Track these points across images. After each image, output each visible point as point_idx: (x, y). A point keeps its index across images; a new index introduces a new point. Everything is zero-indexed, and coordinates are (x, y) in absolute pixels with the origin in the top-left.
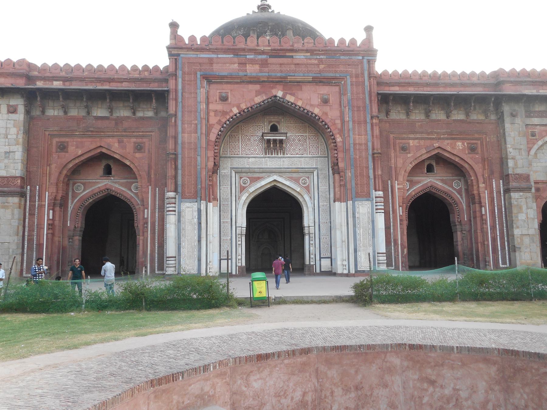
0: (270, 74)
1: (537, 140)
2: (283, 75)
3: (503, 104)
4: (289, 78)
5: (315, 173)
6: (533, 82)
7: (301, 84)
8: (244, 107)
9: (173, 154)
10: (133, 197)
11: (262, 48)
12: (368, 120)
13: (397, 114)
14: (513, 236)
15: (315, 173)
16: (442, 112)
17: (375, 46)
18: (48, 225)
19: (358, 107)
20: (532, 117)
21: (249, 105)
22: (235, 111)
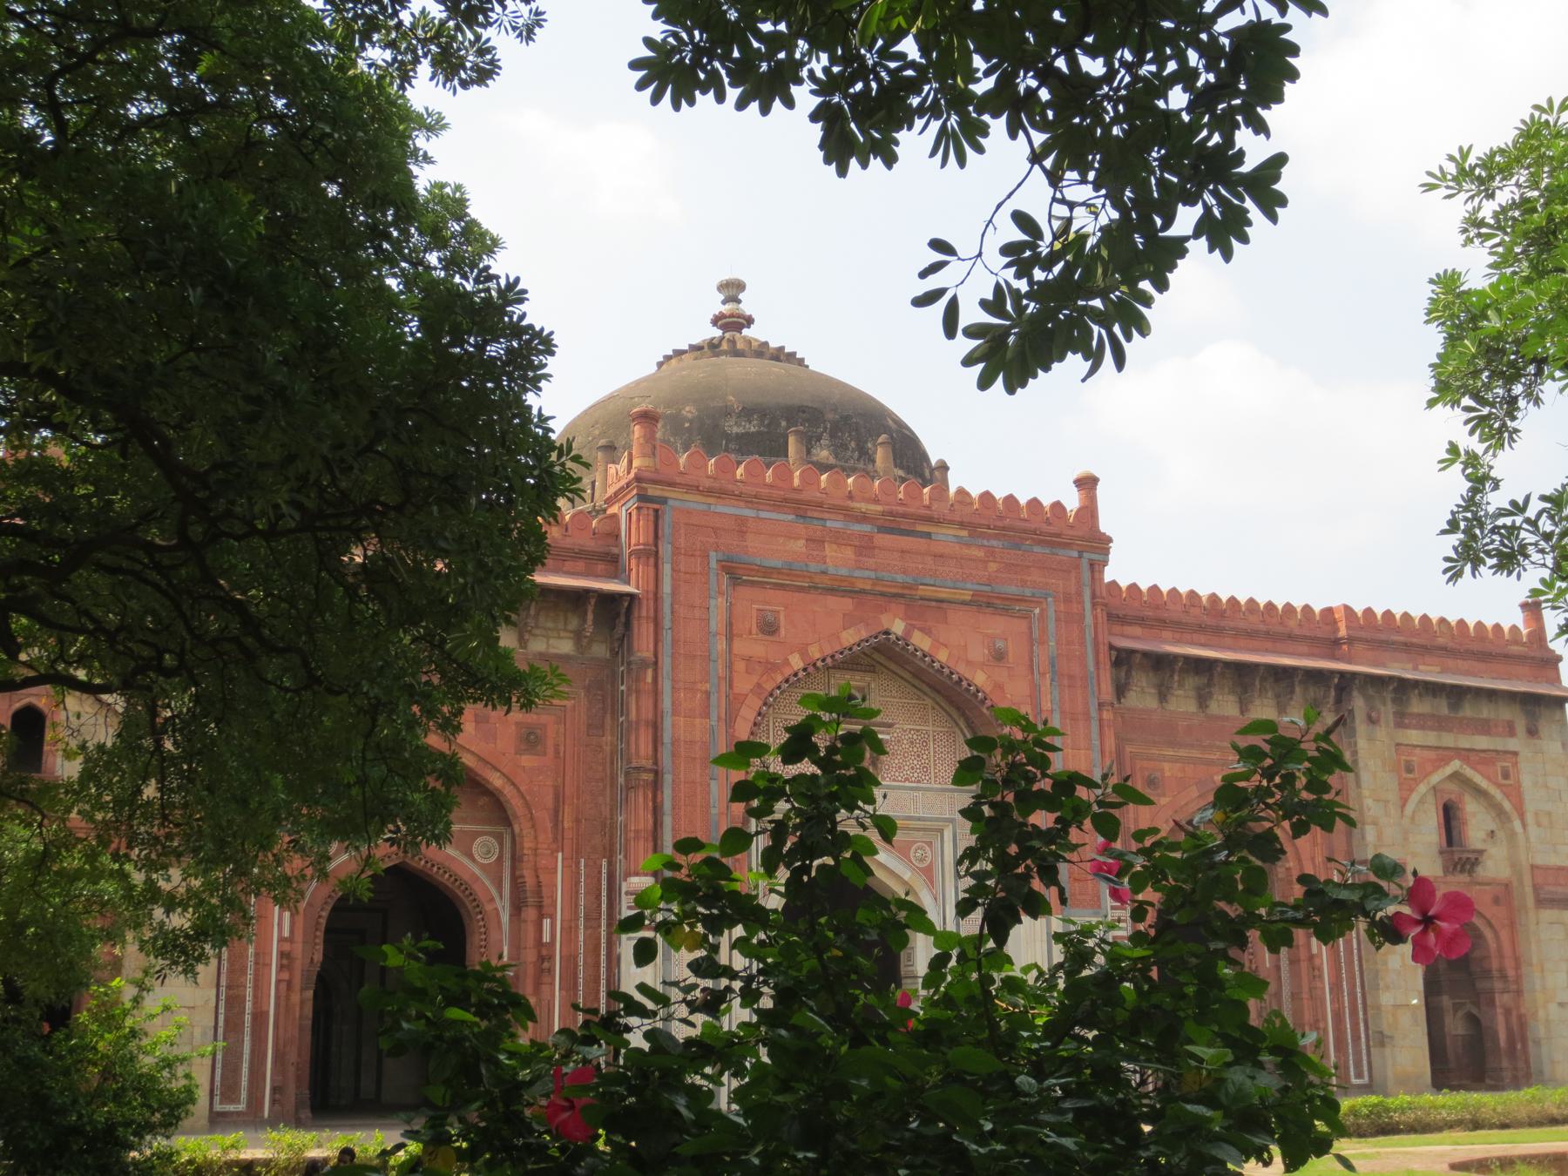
0: (880, 574)
1: (1417, 782)
2: (909, 580)
3: (1355, 693)
4: (923, 591)
5: (948, 834)
6: (1406, 644)
7: (944, 605)
8: (817, 655)
9: (650, 771)
10: (478, 879)
11: (863, 506)
12: (1094, 713)
13: (1142, 697)
14: (1378, 1008)
15: (948, 834)
16: (1232, 698)
17: (1105, 526)
18: (282, 955)
19: (1071, 677)
20: (1407, 727)
21: (828, 651)
22: (797, 662)
